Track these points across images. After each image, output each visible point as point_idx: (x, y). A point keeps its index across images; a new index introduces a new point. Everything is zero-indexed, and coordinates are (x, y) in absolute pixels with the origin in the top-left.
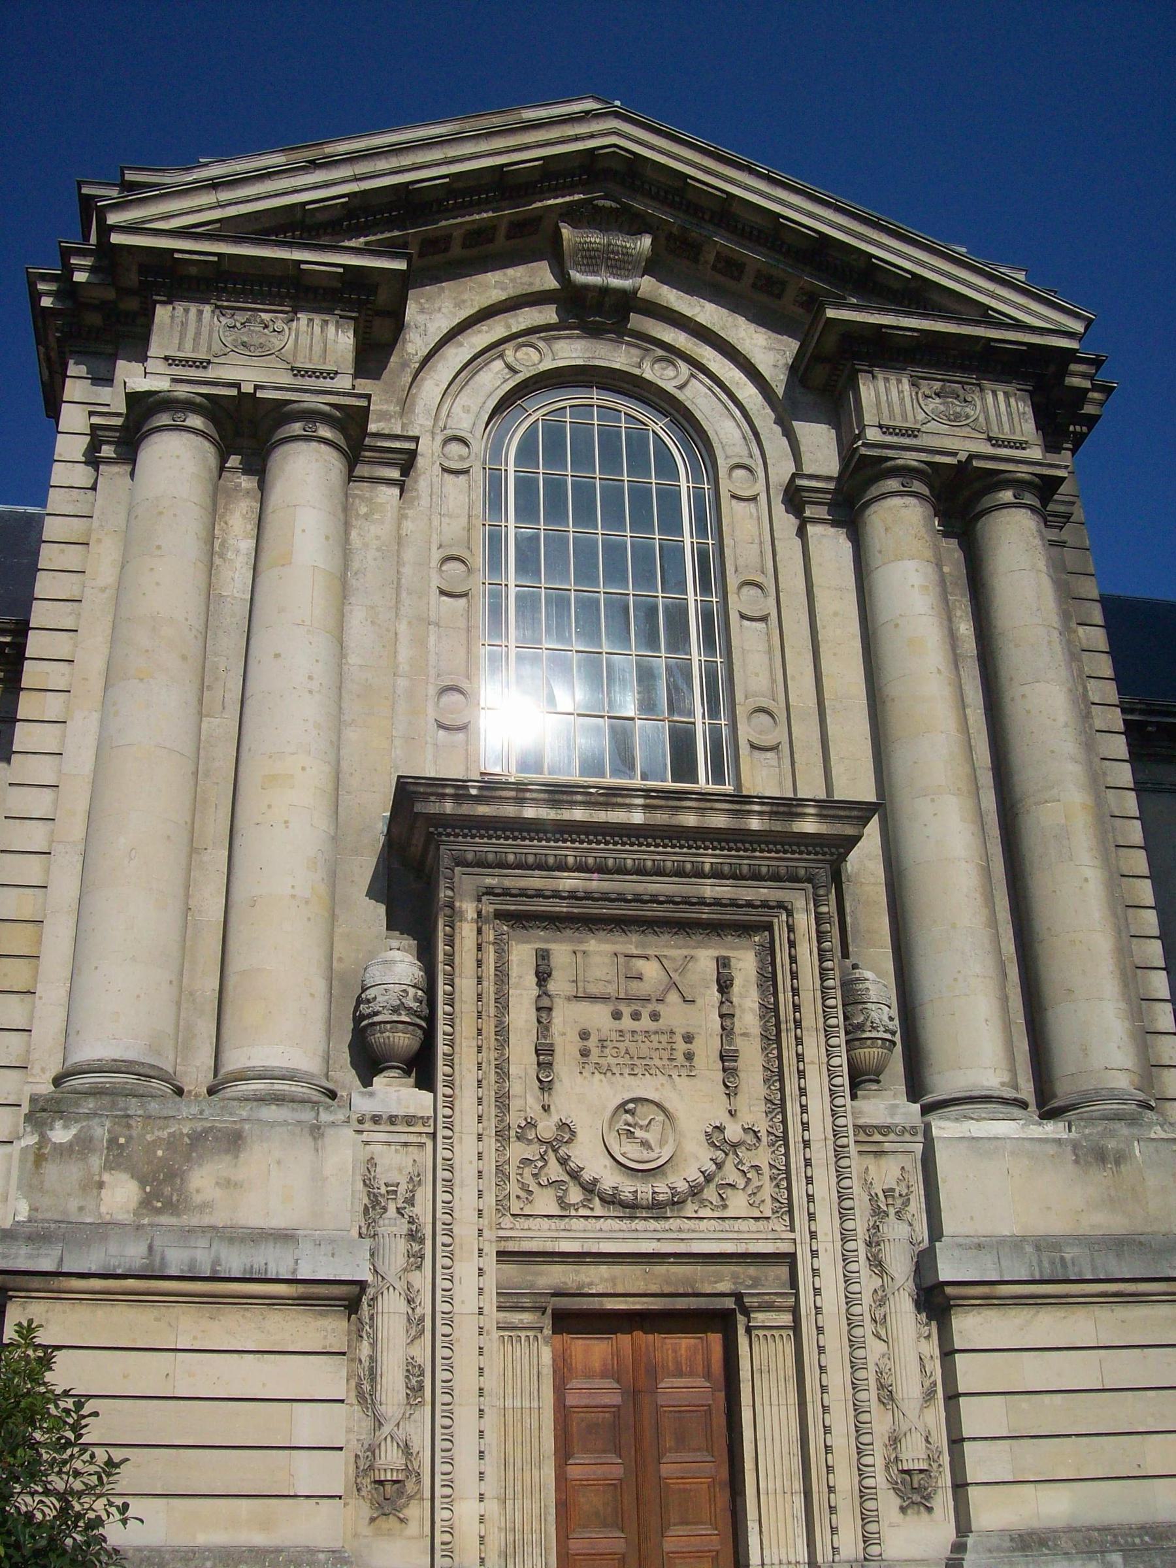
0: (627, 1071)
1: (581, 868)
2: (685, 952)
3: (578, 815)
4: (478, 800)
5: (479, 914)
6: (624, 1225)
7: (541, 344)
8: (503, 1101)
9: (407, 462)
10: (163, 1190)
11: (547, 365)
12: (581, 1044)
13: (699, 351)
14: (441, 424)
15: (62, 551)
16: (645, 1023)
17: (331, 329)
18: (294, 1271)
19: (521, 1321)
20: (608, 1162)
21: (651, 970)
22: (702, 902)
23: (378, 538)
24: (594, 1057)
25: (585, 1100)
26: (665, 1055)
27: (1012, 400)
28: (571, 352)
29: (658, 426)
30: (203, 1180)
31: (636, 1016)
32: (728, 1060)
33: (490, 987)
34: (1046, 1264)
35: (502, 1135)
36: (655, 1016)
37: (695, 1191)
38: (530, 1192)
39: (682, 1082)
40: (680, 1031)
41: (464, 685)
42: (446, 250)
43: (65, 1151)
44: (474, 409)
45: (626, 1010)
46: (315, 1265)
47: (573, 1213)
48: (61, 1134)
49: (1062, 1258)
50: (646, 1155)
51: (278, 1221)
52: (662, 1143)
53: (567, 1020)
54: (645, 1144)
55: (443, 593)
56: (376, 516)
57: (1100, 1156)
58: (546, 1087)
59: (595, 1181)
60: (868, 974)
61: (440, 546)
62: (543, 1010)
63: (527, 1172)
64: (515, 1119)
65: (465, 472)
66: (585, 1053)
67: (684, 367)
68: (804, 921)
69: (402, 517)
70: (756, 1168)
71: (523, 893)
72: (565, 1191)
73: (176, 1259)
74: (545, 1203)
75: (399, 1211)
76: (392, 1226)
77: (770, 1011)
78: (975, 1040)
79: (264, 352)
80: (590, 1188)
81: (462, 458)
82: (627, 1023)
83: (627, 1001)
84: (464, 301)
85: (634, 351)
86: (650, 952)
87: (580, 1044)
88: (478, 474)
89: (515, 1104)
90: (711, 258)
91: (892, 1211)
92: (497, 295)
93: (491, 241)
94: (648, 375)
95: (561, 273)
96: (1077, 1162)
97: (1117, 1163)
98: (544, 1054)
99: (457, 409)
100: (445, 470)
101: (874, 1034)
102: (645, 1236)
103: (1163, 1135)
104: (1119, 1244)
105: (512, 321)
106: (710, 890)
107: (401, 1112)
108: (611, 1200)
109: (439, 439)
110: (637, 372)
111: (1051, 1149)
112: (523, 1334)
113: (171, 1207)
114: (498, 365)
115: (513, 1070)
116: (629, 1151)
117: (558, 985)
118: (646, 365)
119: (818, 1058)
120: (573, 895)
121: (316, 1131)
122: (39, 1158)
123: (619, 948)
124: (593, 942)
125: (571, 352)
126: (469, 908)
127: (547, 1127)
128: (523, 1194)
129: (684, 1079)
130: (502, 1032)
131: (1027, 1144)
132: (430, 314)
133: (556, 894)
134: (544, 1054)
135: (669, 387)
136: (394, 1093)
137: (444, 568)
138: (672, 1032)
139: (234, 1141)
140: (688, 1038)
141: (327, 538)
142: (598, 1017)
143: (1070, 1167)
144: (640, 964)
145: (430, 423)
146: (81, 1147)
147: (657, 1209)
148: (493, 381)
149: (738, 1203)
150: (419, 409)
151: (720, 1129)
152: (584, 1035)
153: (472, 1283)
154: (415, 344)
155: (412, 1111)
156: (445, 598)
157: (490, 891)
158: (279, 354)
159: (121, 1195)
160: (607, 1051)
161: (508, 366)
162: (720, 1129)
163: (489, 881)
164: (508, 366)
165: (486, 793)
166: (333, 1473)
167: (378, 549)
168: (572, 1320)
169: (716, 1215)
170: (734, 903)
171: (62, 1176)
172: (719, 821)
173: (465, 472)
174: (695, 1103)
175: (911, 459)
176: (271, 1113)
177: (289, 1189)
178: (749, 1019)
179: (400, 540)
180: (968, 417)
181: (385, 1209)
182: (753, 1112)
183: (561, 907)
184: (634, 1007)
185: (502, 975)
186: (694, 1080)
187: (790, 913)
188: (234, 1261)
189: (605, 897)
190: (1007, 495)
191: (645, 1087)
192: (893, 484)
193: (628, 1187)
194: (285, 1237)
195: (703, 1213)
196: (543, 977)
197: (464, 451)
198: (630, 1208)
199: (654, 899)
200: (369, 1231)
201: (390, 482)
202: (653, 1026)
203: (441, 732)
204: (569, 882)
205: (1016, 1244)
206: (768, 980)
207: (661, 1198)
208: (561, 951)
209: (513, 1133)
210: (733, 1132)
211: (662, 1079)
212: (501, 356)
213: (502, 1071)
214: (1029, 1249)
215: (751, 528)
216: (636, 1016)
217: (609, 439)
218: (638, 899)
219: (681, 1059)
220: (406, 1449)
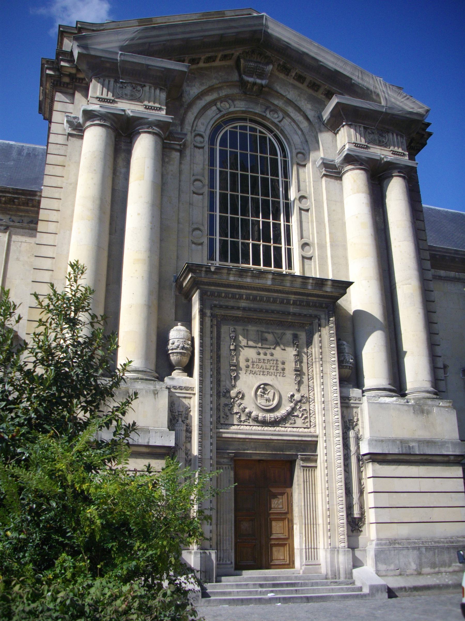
0: (261, 373)
1: (247, 299)
2: (281, 331)
3: (249, 280)
4: (214, 273)
5: (211, 314)
6: (260, 428)
7: (230, 101)
11: (232, 109)
12: (246, 364)
13: (287, 108)
14: (194, 129)
15: (53, 168)
16: (269, 357)
17: (158, 91)
18: (148, 442)
19: (224, 462)
20: (254, 406)
22: (289, 314)
23: (172, 171)
24: (250, 369)
26: (275, 368)
27: (399, 137)
28: (240, 106)
29: (269, 136)
31: (265, 354)
33: (215, 340)
34: (404, 448)
36: (272, 355)
38: (227, 416)
39: (280, 378)
40: (280, 360)
41: (202, 228)
42: (198, 63)
44: (206, 124)
45: (262, 351)
47: (242, 424)
49: (409, 446)
50: (268, 404)
52: (273, 400)
54: (268, 400)
55: (194, 193)
56: (172, 163)
57: (422, 412)
59: (250, 413)
60: (345, 343)
61: (193, 175)
63: (227, 409)
64: (222, 389)
65: (203, 148)
66: (248, 367)
67: (281, 115)
70: (305, 410)
71: (227, 307)
72: (240, 416)
75: (183, 421)
81: (201, 142)
82: (262, 356)
84: (203, 83)
85: (263, 107)
86: (270, 331)
87: (246, 364)
89: (222, 384)
90: (294, 74)
91: (351, 427)
92: (215, 81)
93: (214, 61)
94: (268, 116)
95: (240, 75)
96: (414, 413)
97: (427, 414)
99: (199, 124)
100: (196, 147)
101: (347, 364)
103: (443, 405)
104: (429, 443)
105: (220, 92)
107: (184, 385)
108: (256, 420)
109: (193, 134)
110: (264, 114)
111: (406, 408)
112: (224, 466)
114: (214, 108)
115: (222, 371)
116: (261, 402)
118: (268, 112)
120: (244, 309)
123: (258, 329)
124: (250, 326)
125: (240, 106)
126: (208, 312)
128: (225, 416)
129: (281, 377)
131: (398, 406)
133: (238, 308)
135: (276, 121)
137: (195, 183)
138: (277, 360)
140: (283, 363)
141: (156, 171)
143: (412, 414)
144: (266, 335)
145: (190, 128)
149: (299, 422)
150: (186, 122)
151: (293, 396)
152: (247, 360)
154: (187, 99)
155: (187, 385)
156: (195, 195)
157: (215, 306)
160: (255, 366)
161: (218, 109)
162: (293, 396)
163: (215, 302)
164: (218, 109)
165: (217, 271)
167: (172, 175)
169: (291, 426)
170: (300, 315)
173: (203, 148)
179: (180, 172)
180: (383, 142)
181: (178, 421)
183: (239, 313)
184: (264, 350)
186: (284, 378)
187: (319, 320)
189: (255, 310)
193: (261, 415)
195: (286, 426)
197: (202, 140)
199: (273, 312)
201: (176, 150)
202: (270, 358)
203: (193, 245)
204: (243, 304)
207: (273, 419)
209: (221, 394)
211: (273, 377)
212: (215, 105)
214: (398, 442)
216: (265, 354)
217: (253, 138)
218: (267, 311)
219: (280, 370)
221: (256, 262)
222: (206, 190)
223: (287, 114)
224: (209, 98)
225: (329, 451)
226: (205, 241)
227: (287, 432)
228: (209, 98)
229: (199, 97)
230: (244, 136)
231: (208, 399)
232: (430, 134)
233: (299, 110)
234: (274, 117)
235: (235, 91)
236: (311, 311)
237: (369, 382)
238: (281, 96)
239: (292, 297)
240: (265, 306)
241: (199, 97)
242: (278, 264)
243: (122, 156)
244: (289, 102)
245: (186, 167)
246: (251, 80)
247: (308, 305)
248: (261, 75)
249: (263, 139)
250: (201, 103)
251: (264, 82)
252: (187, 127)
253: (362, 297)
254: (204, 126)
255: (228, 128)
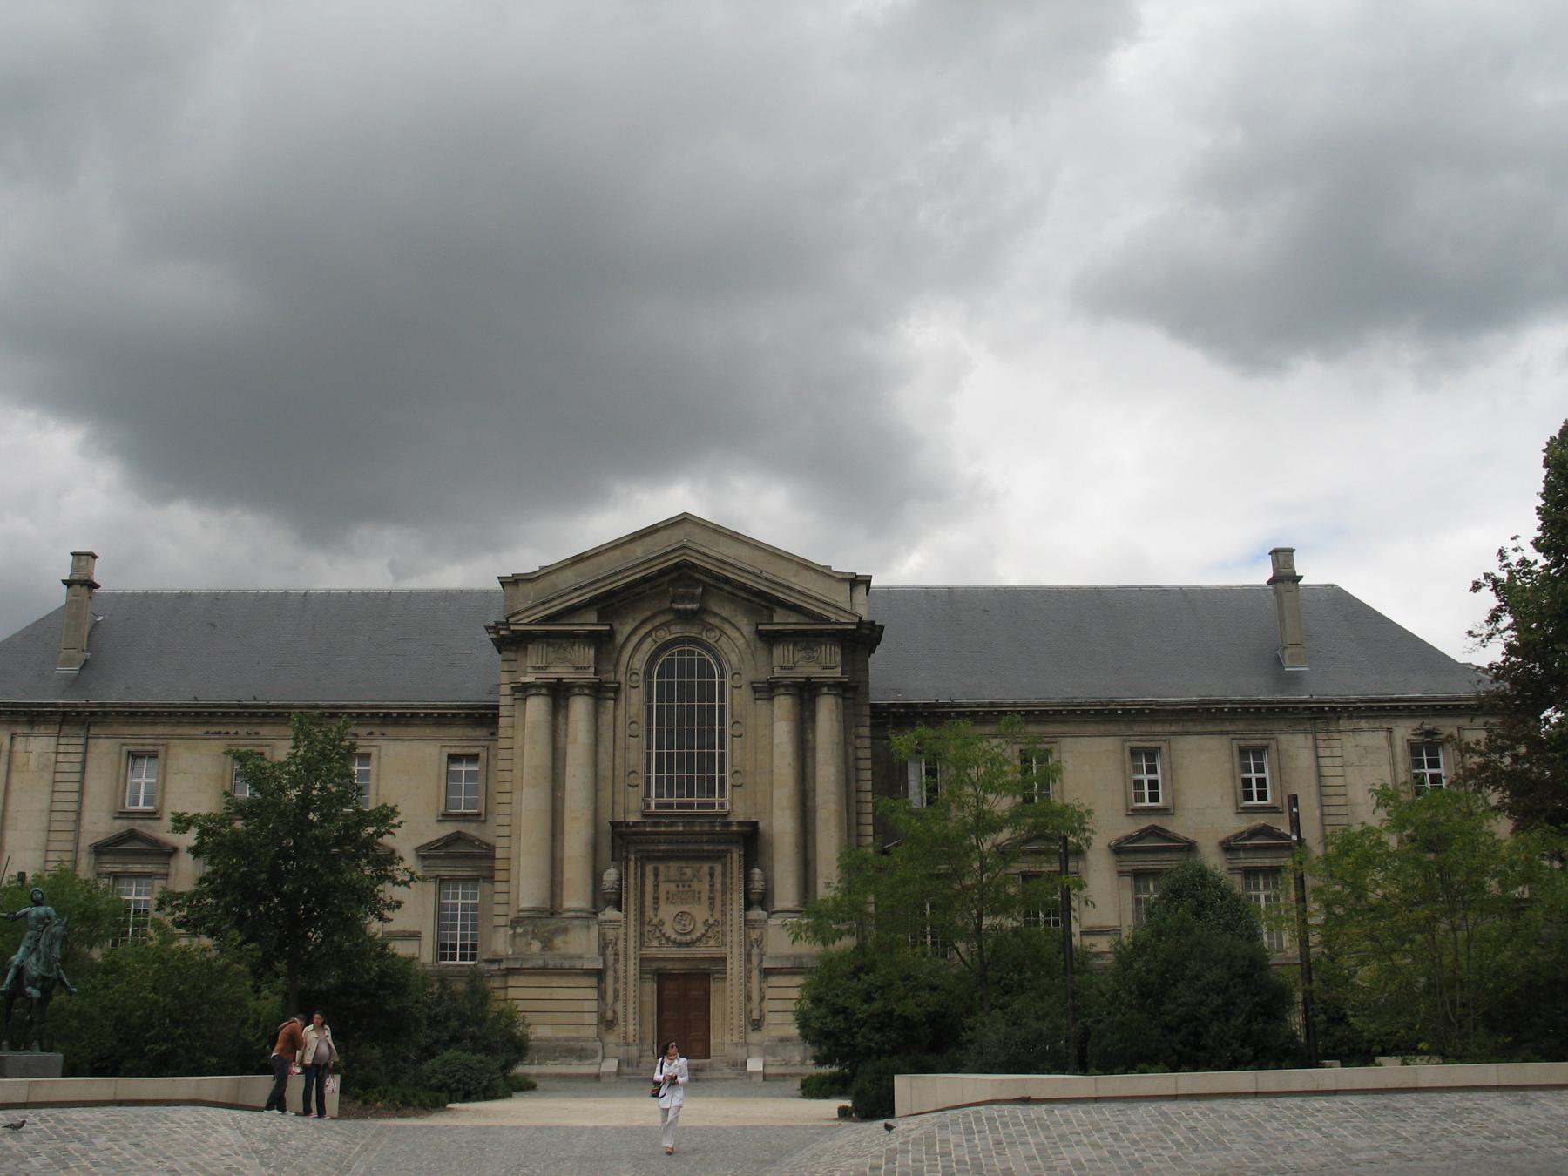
8: (642, 913)
9: (617, 690)
10: (547, 945)
21: (689, 872)
25: (667, 912)
28: (677, 631)
29: (708, 657)
30: (558, 942)
32: (712, 900)
35: (642, 924)
37: (699, 939)
43: (521, 935)
46: (588, 965)
48: (519, 930)
51: (579, 952)
53: (663, 888)
58: (656, 909)
62: (656, 886)
67: (718, 633)
68: (735, 856)
69: (615, 709)
73: (551, 964)
74: (655, 943)
76: (610, 951)
77: (724, 884)
78: (786, 893)
79: (564, 660)
80: (668, 939)
83: (682, 881)
88: (642, 685)
92: (648, 613)
98: (656, 900)
102: (683, 953)
106: (706, 847)
108: (674, 942)
113: (550, 949)
116: (679, 928)
117: (661, 878)
119: (738, 899)
121: (588, 927)
122: (514, 936)
125: (677, 631)
126: (632, 857)
127: (655, 921)
130: (643, 893)
132: (623, 630)
134: (656, 900)
136: (610, 913)
139: (565, 930)
142: (672, 887)
146: (525, 933)
147: (688, 944)
148: (648, 647)
149: (712, 942)
153: (633, 968)
154: (620, 639)
158: (570, 661)
159: (536, 946)
166: (593, 1018)
168: (662, 977)
171: (520, 942)
172: (706, 828)
174: (700, 912)
175: (787, 681)
176: (576, 922)
177: (581, 944)
178: (718, 886)
182: (718, 915)
185: (643, 875)
188: (566, 964)
190: (825, 690)
191: (685, 908)
192: (782, 690)
193: (679, 938)
194: (580, 957)
196: (656, 875)
198: (680, 944)
200: (602, 953)
204: (663, 847)
205: (788, 957)
206: (724, 874)
208: (662, 867)
210: (711, 921)
213: (643, 905)
215: (736, 700)
217: (691, 661)
220: (614, 1012)
221: (691, 794)
222: (642, 732)
223: (723, 632)
224: (642, 632)
225: (735, 966)
226: (642, 782)
227: (700, 952)
228: (642, 632)
229: (633, 633)
230: (681, 662)
231: (632, 929)
232: (882, 628)
233: (733, 625)
234: (709, 637)
235: (668, 617)
236: (723, 847)
237: (779, 904)
238: (716, 614)
239: (705, 838)
240: (681, 847)
241: (633, 633)
242: (712, 792)
243: (562, 712)
244: (724, 619)
245: (621, 712)
246: (681, 606)
247: (719, 842)
248: (692, 599)
249: (701, 661)
250: (635, 639)
251: (695, 606)
252: (622, 669)
253: (781, 826)
254: (639, 663)
255: (665, 657)
